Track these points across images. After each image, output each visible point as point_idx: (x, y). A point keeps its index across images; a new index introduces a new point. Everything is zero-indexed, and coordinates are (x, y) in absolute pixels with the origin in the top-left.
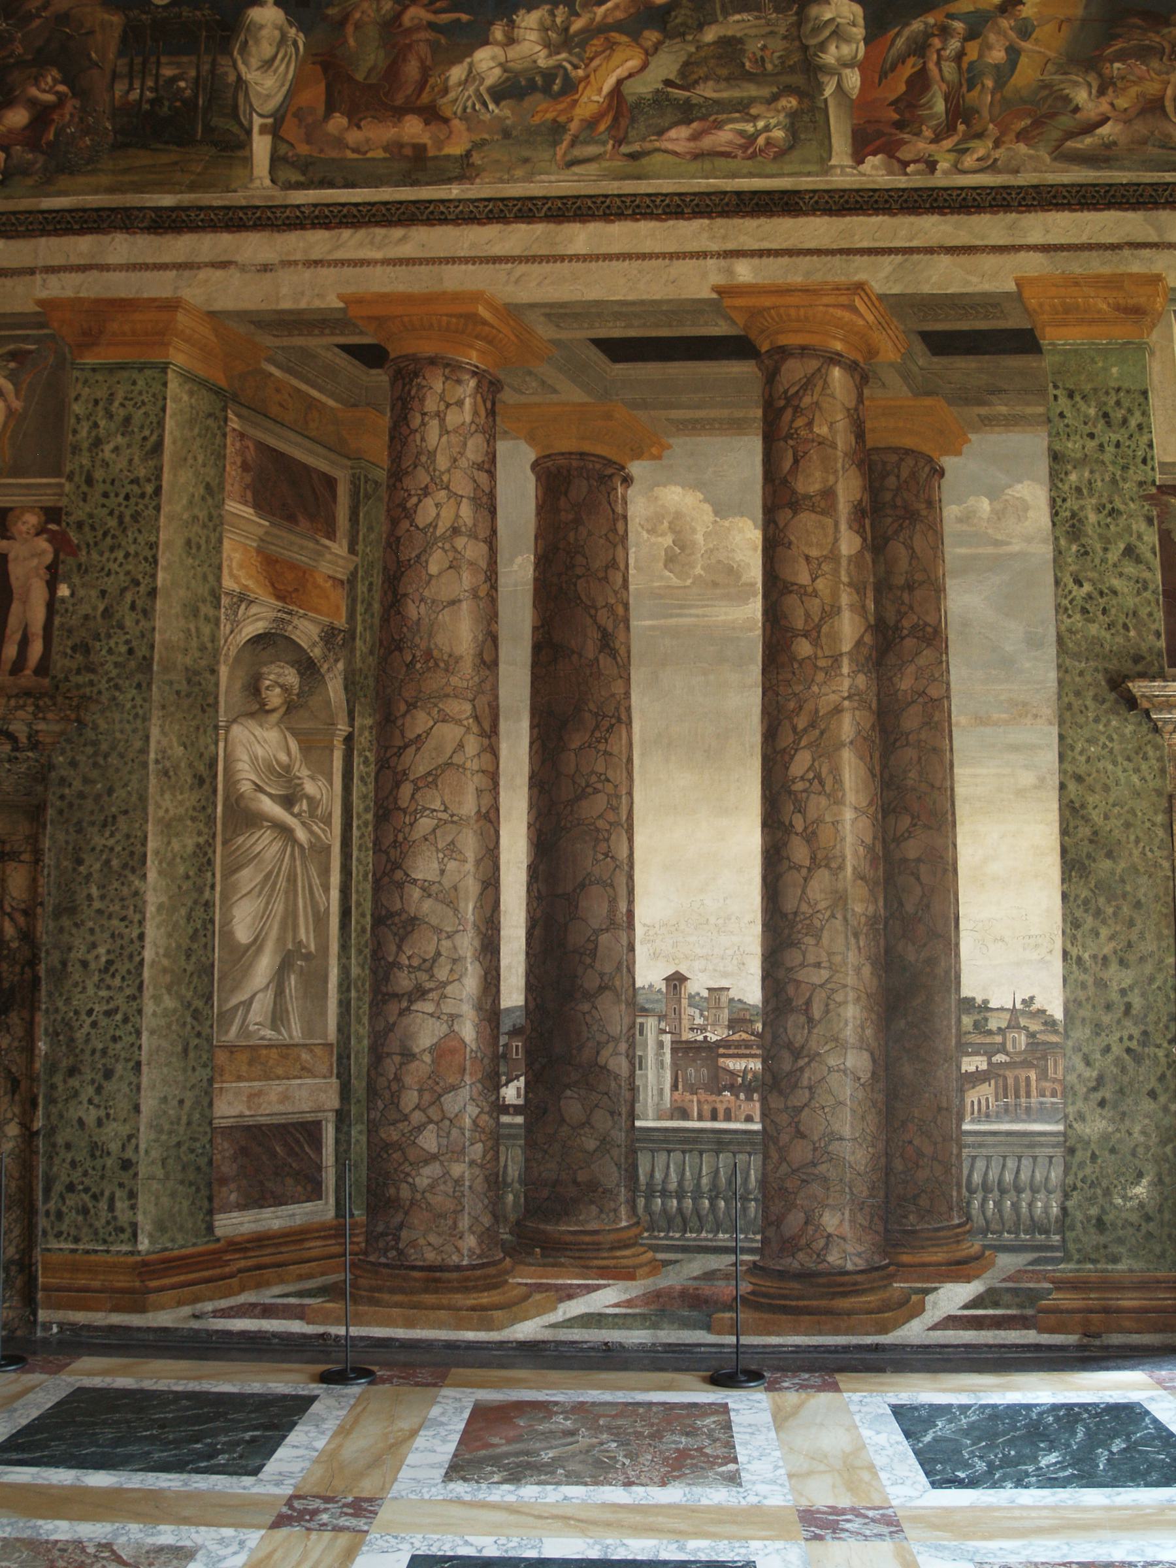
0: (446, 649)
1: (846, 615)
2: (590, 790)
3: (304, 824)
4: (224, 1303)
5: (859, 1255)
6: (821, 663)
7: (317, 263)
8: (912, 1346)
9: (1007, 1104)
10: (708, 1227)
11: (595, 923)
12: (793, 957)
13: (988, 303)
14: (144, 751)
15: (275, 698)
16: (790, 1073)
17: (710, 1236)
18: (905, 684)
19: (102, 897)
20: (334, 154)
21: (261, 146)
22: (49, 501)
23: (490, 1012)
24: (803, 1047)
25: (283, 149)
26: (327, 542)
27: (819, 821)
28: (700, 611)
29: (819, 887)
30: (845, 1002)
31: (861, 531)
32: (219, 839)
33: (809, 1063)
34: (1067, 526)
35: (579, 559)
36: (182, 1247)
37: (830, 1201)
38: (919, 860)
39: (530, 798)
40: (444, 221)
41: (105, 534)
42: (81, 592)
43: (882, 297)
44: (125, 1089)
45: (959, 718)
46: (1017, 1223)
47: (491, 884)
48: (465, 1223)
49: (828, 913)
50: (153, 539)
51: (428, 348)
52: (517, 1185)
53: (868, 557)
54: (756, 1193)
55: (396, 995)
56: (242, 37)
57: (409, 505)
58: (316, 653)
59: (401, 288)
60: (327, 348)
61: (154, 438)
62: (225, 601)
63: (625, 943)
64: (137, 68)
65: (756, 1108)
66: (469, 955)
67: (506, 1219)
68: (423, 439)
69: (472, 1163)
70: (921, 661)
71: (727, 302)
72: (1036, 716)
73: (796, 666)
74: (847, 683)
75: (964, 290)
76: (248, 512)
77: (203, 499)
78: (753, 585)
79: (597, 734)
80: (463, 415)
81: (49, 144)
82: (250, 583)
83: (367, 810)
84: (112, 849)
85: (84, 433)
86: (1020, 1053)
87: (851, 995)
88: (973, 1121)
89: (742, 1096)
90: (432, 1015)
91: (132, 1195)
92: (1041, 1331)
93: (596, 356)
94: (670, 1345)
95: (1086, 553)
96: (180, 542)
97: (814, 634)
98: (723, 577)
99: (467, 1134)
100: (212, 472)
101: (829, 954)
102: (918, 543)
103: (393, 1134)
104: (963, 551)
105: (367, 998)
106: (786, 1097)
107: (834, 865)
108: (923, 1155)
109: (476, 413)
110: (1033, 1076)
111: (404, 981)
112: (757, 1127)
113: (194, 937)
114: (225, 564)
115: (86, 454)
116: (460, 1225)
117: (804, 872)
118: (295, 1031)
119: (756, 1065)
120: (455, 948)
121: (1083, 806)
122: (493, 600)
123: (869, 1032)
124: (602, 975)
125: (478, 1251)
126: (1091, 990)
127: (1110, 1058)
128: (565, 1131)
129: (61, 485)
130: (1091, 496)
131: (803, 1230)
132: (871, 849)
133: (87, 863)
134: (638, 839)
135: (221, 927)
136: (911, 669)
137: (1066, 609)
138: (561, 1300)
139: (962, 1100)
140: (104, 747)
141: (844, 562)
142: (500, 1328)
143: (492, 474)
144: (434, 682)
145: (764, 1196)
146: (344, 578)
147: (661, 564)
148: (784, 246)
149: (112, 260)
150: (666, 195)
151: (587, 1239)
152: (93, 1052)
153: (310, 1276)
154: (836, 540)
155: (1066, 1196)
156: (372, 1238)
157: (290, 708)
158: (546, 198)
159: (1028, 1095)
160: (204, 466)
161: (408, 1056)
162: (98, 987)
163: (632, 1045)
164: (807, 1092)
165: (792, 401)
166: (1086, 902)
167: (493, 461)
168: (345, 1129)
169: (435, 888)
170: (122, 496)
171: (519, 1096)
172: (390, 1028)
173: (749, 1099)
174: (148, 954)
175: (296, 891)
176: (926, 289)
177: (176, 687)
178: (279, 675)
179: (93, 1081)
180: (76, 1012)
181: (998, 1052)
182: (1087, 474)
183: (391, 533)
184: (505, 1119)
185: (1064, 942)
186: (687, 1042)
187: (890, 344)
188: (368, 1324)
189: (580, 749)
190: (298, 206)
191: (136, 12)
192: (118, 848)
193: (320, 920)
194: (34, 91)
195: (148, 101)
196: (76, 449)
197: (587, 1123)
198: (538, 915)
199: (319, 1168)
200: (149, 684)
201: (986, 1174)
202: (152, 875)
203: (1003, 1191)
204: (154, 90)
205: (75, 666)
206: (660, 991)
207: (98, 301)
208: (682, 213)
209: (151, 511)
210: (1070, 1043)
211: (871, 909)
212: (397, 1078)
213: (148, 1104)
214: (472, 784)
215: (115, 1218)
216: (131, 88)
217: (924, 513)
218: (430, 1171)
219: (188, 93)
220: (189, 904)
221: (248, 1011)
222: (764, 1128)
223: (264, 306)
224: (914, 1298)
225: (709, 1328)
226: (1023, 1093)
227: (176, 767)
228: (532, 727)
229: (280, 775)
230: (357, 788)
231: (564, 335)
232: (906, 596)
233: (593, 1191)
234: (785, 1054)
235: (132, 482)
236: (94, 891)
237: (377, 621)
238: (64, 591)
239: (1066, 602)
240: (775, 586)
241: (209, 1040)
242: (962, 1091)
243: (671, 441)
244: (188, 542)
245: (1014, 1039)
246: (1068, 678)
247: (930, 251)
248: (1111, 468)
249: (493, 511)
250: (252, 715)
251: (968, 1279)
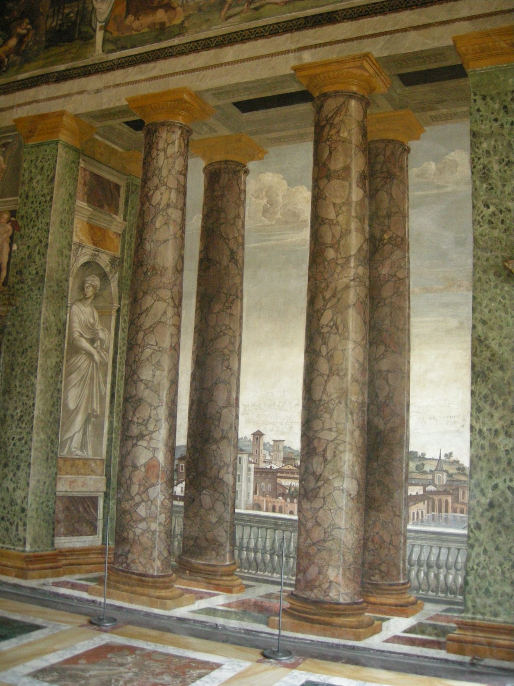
0: (161, 265)
1: (354, 234)
2: (222, 334)
3: (98, 352)
4: (56, 580)
5: (347, 594)
6: (340, 261)
7: (118, 85)
8: (374, 650)
9: (433, 515)
10: (269, 569)
11: (221, 403)
12: (317, 425)
13: (438, 53)
14: (39, 319)
15: (90, 292)
16: (313, 490)
17: (270, 574)
18: (384, 271)
19: (20, 386)
20: (127, 34)
21: (99, 36)
22: (12, 207)
23: (172, 449)
24: (321, 475)
25: (108, 35)
26: (114, 216)
27: (335, 349)
28: (278, 237)
29: (333, 387)
30: (344, 451)
31: (363, 188)
32: (65, 359)
33: (324, 484)
34: (481, 173)
35: (223, 215)
36: (42, 551)
37: (332, 563)
38: (388, 371)
39: (194, 338)
40: (171, 56)
41: (31, 221)
42: (21, 247)
43: (378, 59)
44: (24, 475)
45: (414, 288)
46: (437, 587)
47: (174, 382)
48: (156, 554)
49: (337, 401)
50: (48, 221)
51: (160, 118)
52: (179, 537)
53: (367, 201)
54: (293, 554)
55: (131, 437)
57: (149, 195)
58: (108, 269)
59: (152, 91)
60: (120, 124)
61: (51, 175)
62: (73, 247)
63: (234, 414)
65: (295, 507)
66: (163, 418)
67: (174, 554)
68: (157, 162)
69: (160, 524)
70: (394, 257)
71: (299, 74)
72: (459, 286)
73: (326, 263)
74: (353, 271)
75: (424, 48)
76: (84, 205)
77: (68, 200)
78: (305, 221)
79: (227, 305)
80: (174, 149)
82: (83, 238)
83: (124, 345)
84: (25, 364)
85: (26, 176)
86: (443, 485)
87: (348, 447)
88: (414, 524)
89: (288, 500)
90: (146, 448)
91: (25, 525)
92: (449, 651)
93: (235, 110)
94: (248, 630)
95: (492, 188)
96: (58, 221)
97: (337, 246)
98: (291, 219)
99: (159, 509)
100: (72, 188)
101: (337, 424)
102: (394, 191)
103: (127, 506)
104: (420, 193)
105: (119, 438)
106: (311, 502)
107: (341, 374)
108: (384, 542)
109: (180, 147)
110: (450, 499)
111: (135, 431)
112: (295, 517)
113: (53, 406)
114: (74, 230)
115: (27, 185)
116: (154, 554)
117: (325, 377)
118: (89, 453)
119: (296, 483)
120: (157, 414)
121: (486, 339)
122: (183, 238)
123: (357, 468)
124: (223, 431)
125: (161, 569)
126: (487, 449)
127: (498, 492)
128: (202, 511)
129: (17, 200)
130: (495, 155)
131: (317, 577)
132: (362, 365)
133: (16, 370)
134: (243, 359)
135: (64, 401)
136: (388, 262)
137: (479, 222)
138: (197, 599)
139: (408, 512)
140: (25, 317)
141: (354, 205)
142: (169, 609)
143: (185, 176)
144: (155, 281)
145: (298, 556)
146: (121, 233)
147: (261, 214)
148: (328, 40)
149: (41, 97)
150: (271, 25)
151: (211, 569)
152: (14, 457)
153: (91, 572)
154: (350, 193)
155: (467, 574)
156: (117, 556)
157: (96, 296)
158: (216, 37)
159: (447, 511)
160: (69, 185)
161: (135, 467)
162: (17, 427)
163: (235, 469)
164: (322, 500)
165: (329, 121)
166: (486, 397)
167: (186, 169)
168: (108, 502)
169: (150, 384)
170: (38, 202)
171: (182, 491)
172: (128, 453)
173: (292, 502)
174: (36, 413)
175: (93, 384)
176: (403, 51)
177: (53, 288)
178: (92, 281)
179: (13, 470)
180: (8, 439)
181: (430, 484)
182: (493, 143)
183: (141, 210)
184: (176, 503)
185: (471, 420)
186: (262, 469)
187: (382, 83)
188: (113, 599)
189: (218, 312)
190: (112, 61)
192: (27, 364)
193: (102, 399)
196: (23, 183)
197: (212, 508)
198: (195, 399)
199: (96, 520)
200: (43, 288)
201: (420, 555)
202: (39, 376)
203: (429, 567)
205: (17, 281)
206: (250, 440)
207: (34, 117)
208: (278, 32)
209: (48, 208)
210: (473, 481)
211: (361, 398)
212: (130, 478)
213: (32, 483)
214: (170, 330)
215: (18, 534)
217: (398, 174)
218: (142, 525)
219: (74, 18)
220: (52, 390)
221: (72, 442)
222: (299, 518)
223: (96, 109)
224: (376, 623)
225: (267, 624)
226: (443, 509)
227: (51, 326)
228: (197, 302)
229: (90, 329)
230: (121, 334)
231: (220, 103)
232: (386, 221)
233: (214, 545)
234: (311, 478)
235: (42, 196)
236: (18, 384)
237: (133, 253)
238: (15, 247)
239: (479, 218)
240: (318, 220)
241: (56, 454)
242: (407, 506)
243: (268, 150)
244: (61, 222)
245: (439, 477)
246: (479, 263)
247: (405, 30)
248: (508, 138)
249: (185, 194)
250: (80, 300)
251: (407, 615)
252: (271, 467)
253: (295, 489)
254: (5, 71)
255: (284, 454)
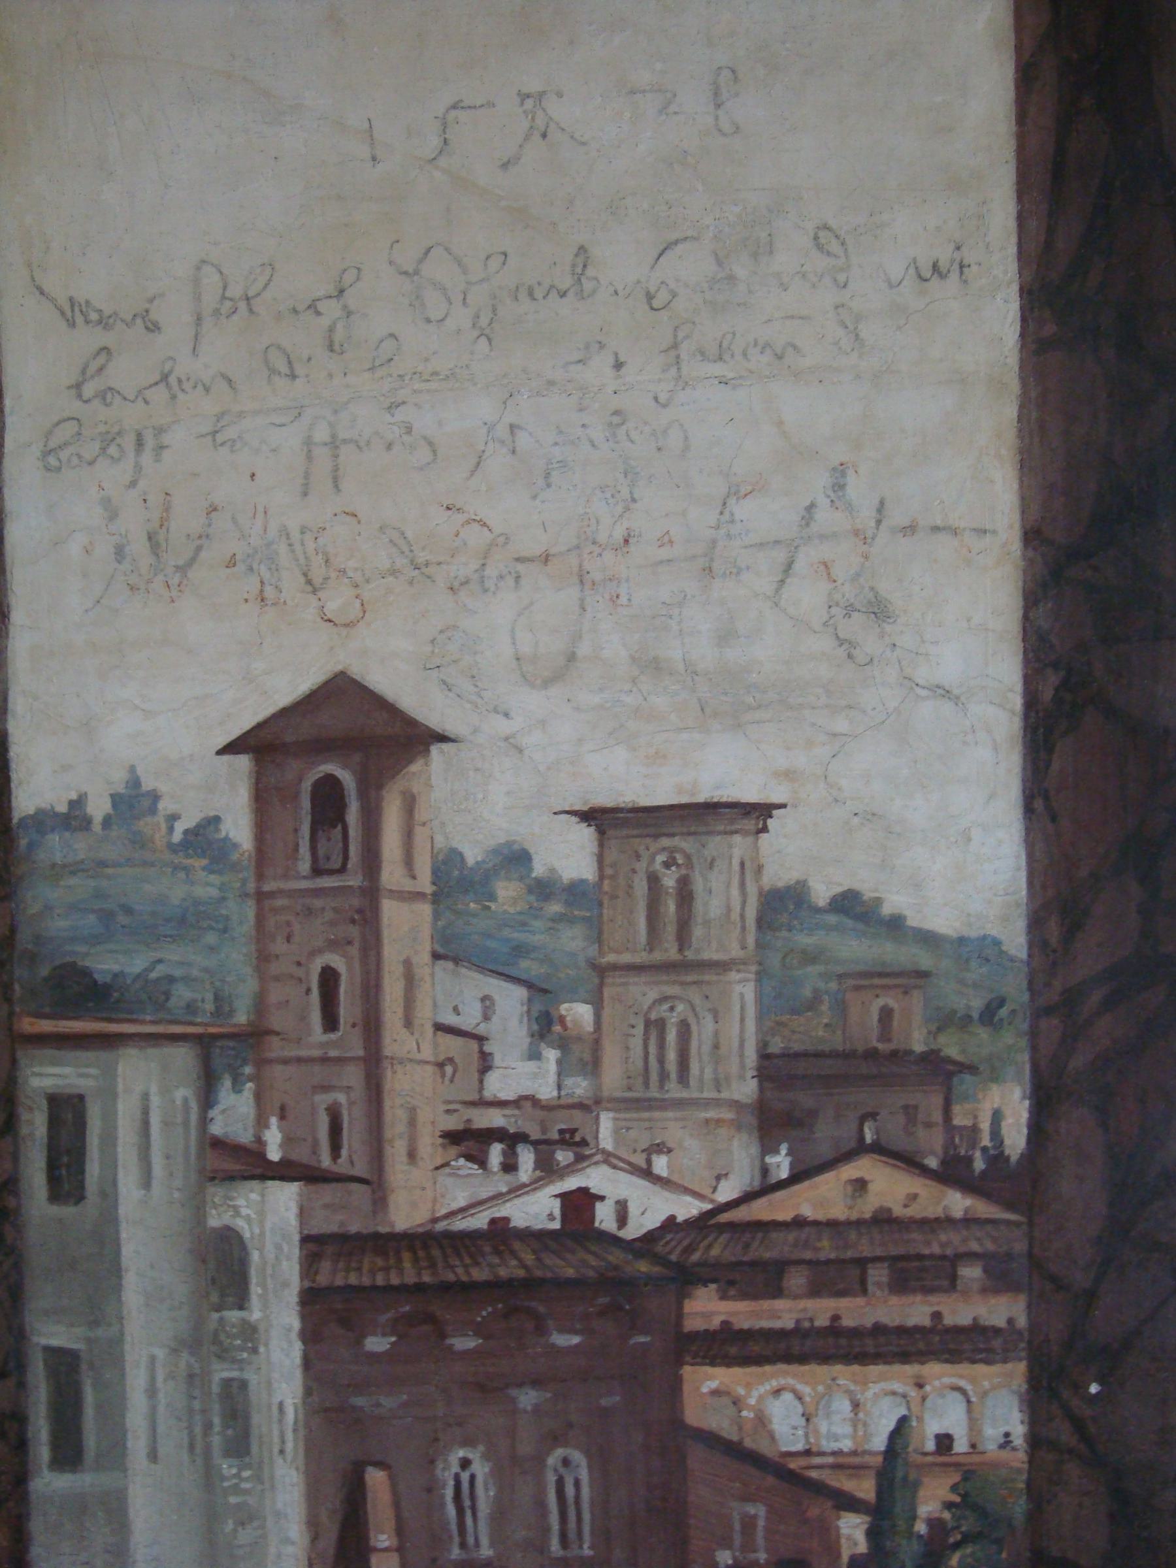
119: (979, 1413)
186: (427, 1242)
206: (203, 839)
252: (579, 1204)
253: (967, 1500)
255: (778, 1004)
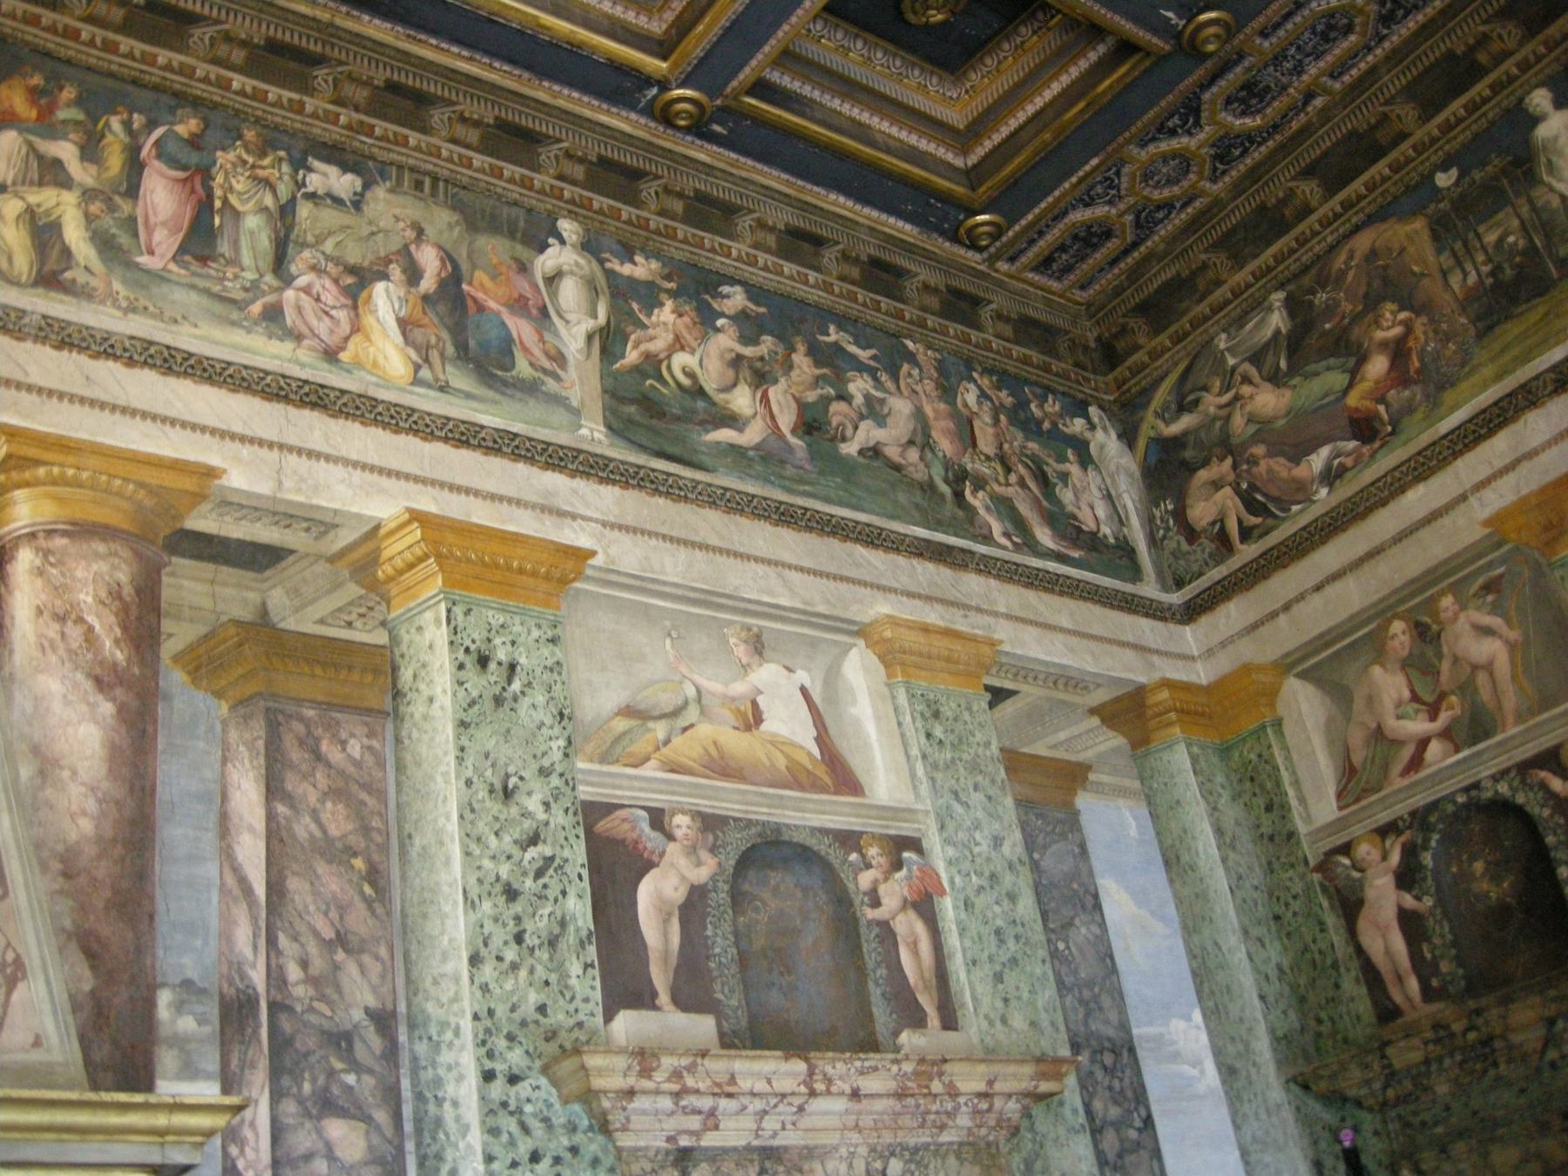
56: (1543, 159)
64: (1461, 253)
81: (1418, 372)
149: (1535, 442)
191: (1432, 206)
194: (1380, 335)
195: (1488, 276)
204: (1490, 260)
207: (1543, 490)
216: (1465, 274)
254: (1391, 434)
